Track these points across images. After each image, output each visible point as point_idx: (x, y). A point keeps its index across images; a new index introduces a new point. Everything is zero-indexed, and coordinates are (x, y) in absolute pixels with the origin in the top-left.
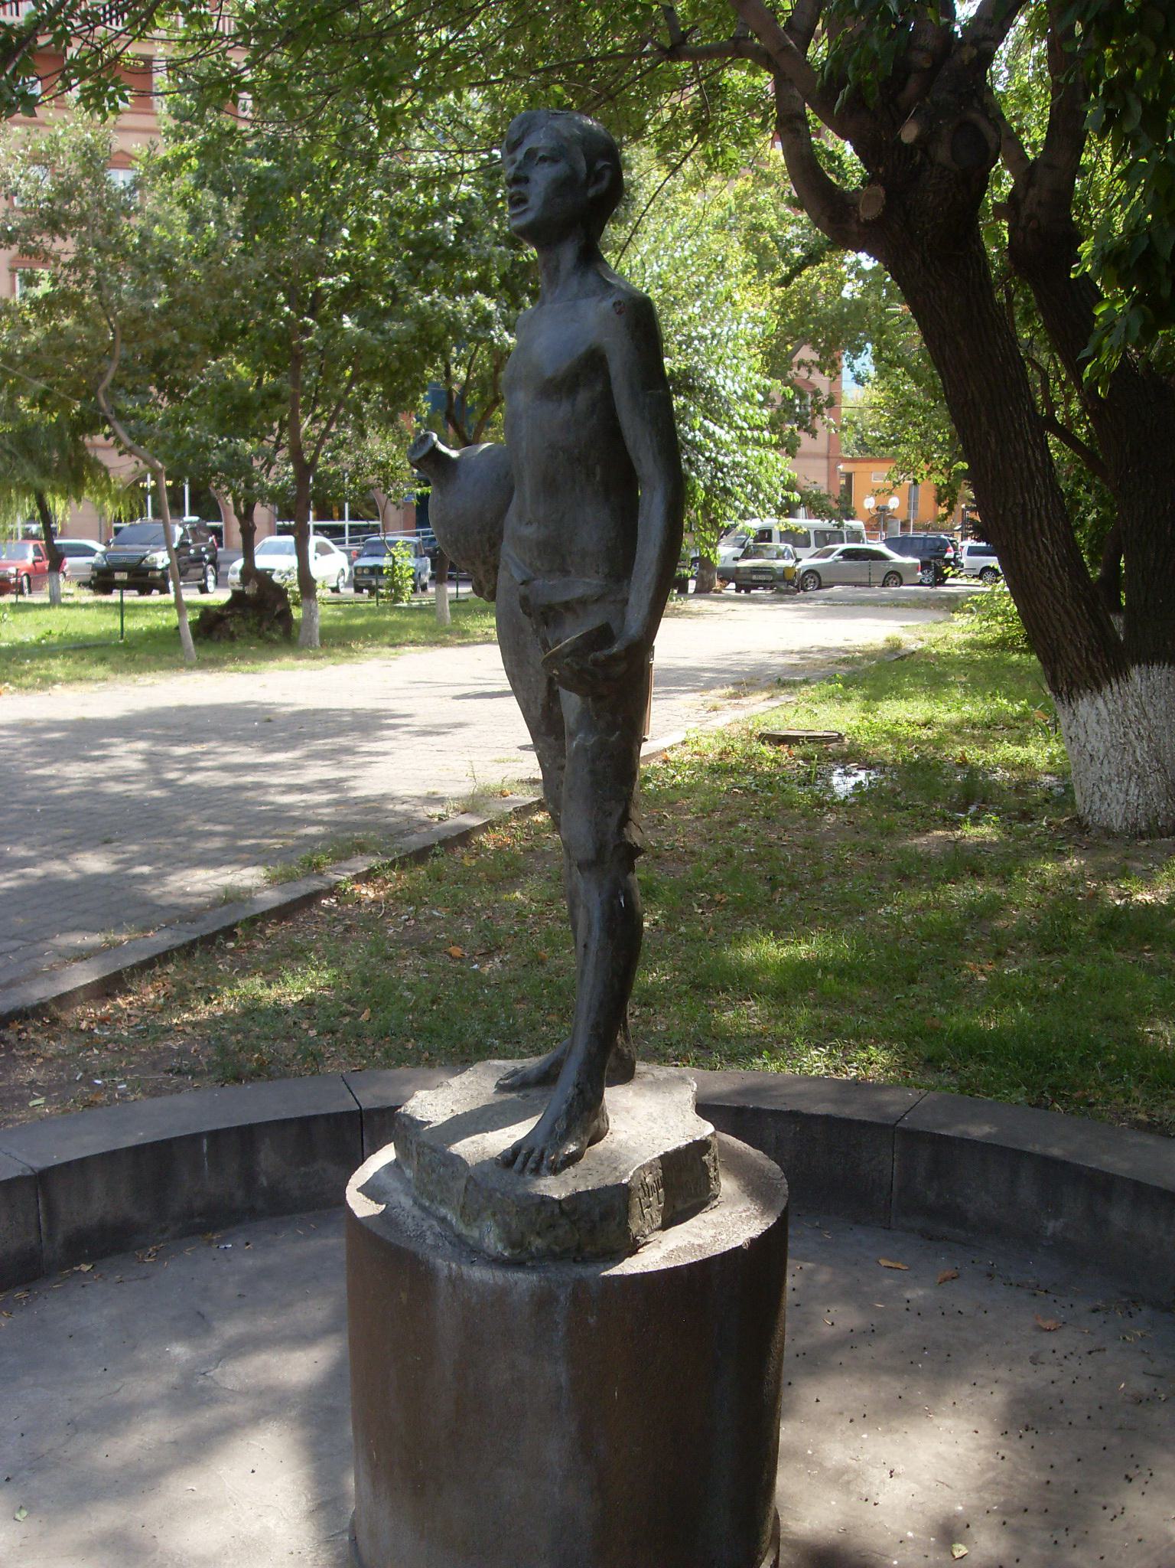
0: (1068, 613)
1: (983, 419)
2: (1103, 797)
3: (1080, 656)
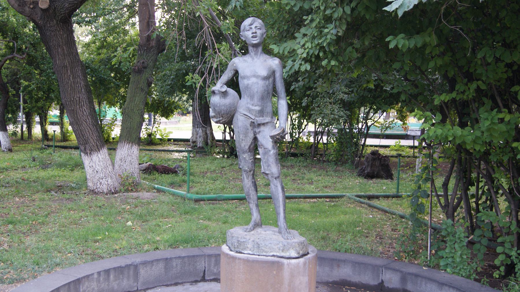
0: (91, 129)
1: (69, 71)
2: (101, 183)
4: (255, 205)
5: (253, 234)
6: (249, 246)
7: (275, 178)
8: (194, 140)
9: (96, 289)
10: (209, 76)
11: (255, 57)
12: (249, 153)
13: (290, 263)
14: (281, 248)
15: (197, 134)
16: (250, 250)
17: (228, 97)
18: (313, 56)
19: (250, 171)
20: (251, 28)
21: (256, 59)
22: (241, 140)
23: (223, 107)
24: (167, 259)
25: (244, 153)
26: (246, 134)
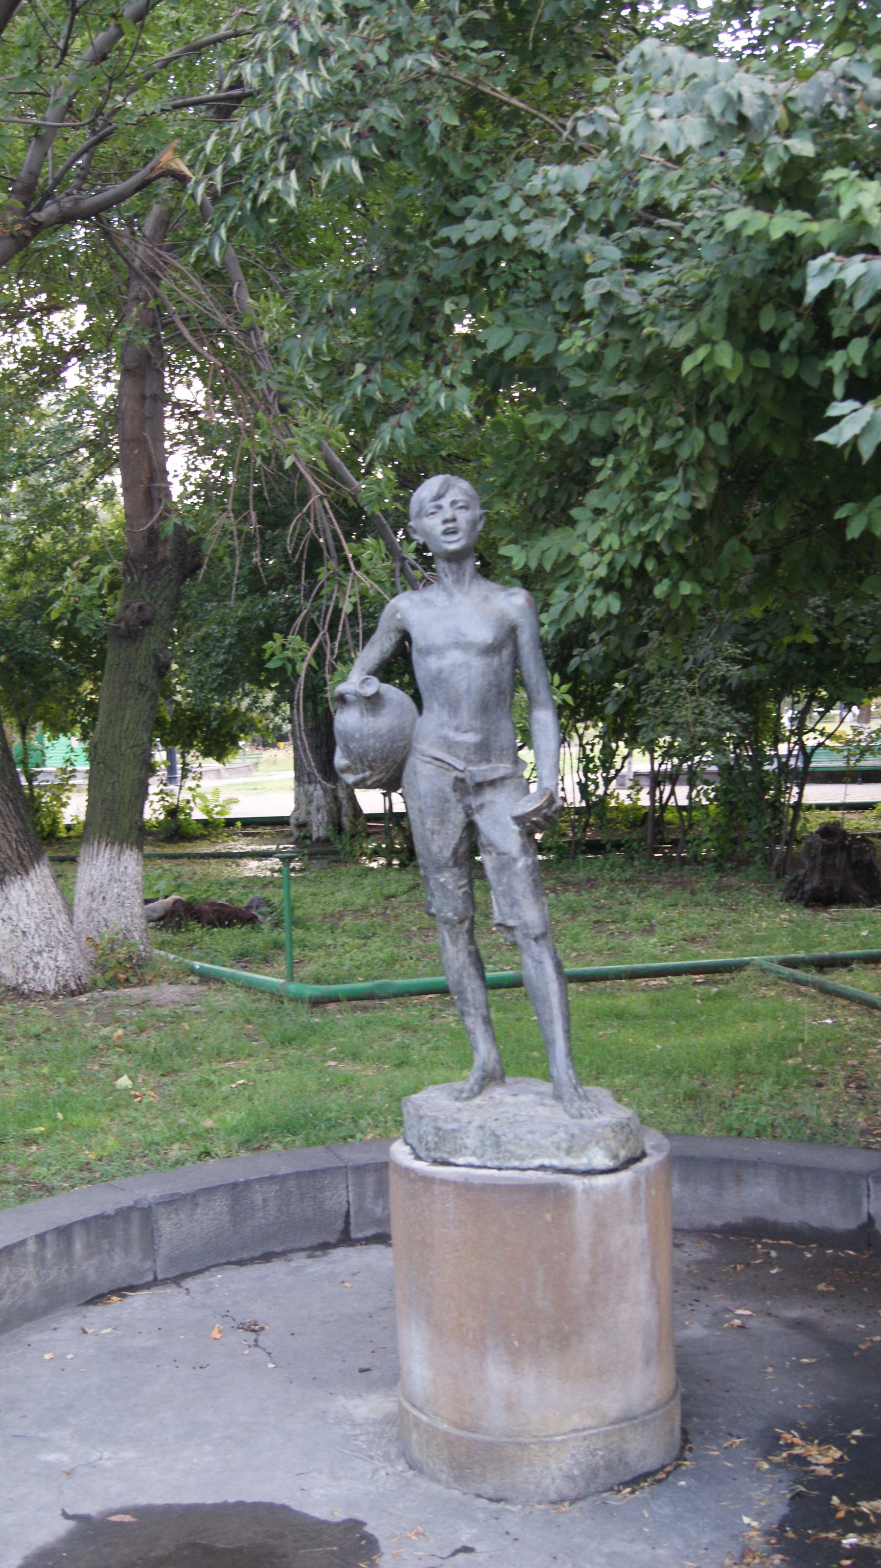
2: (36, 967)
3: (11, 848)
4: (480, 1020)
5: (480, 1107)
6: (471, 1142)
7: (536, 939)
8: (303, 818)
9: (35, 1284)
10: (333, 639)
11: (455, 591)
12: (456, 870)
13: (591, 1187)
14: (564, 1145)
15: (310, 802)
16: (474, 1154)
17: (385, 712)
18: (627, 572)
19: (461, 922)
20: (440, 507)
21: (458, 597)
23: (372, 741)
24: (235, 1185)
25: (439, 869)
26: (442, 816)
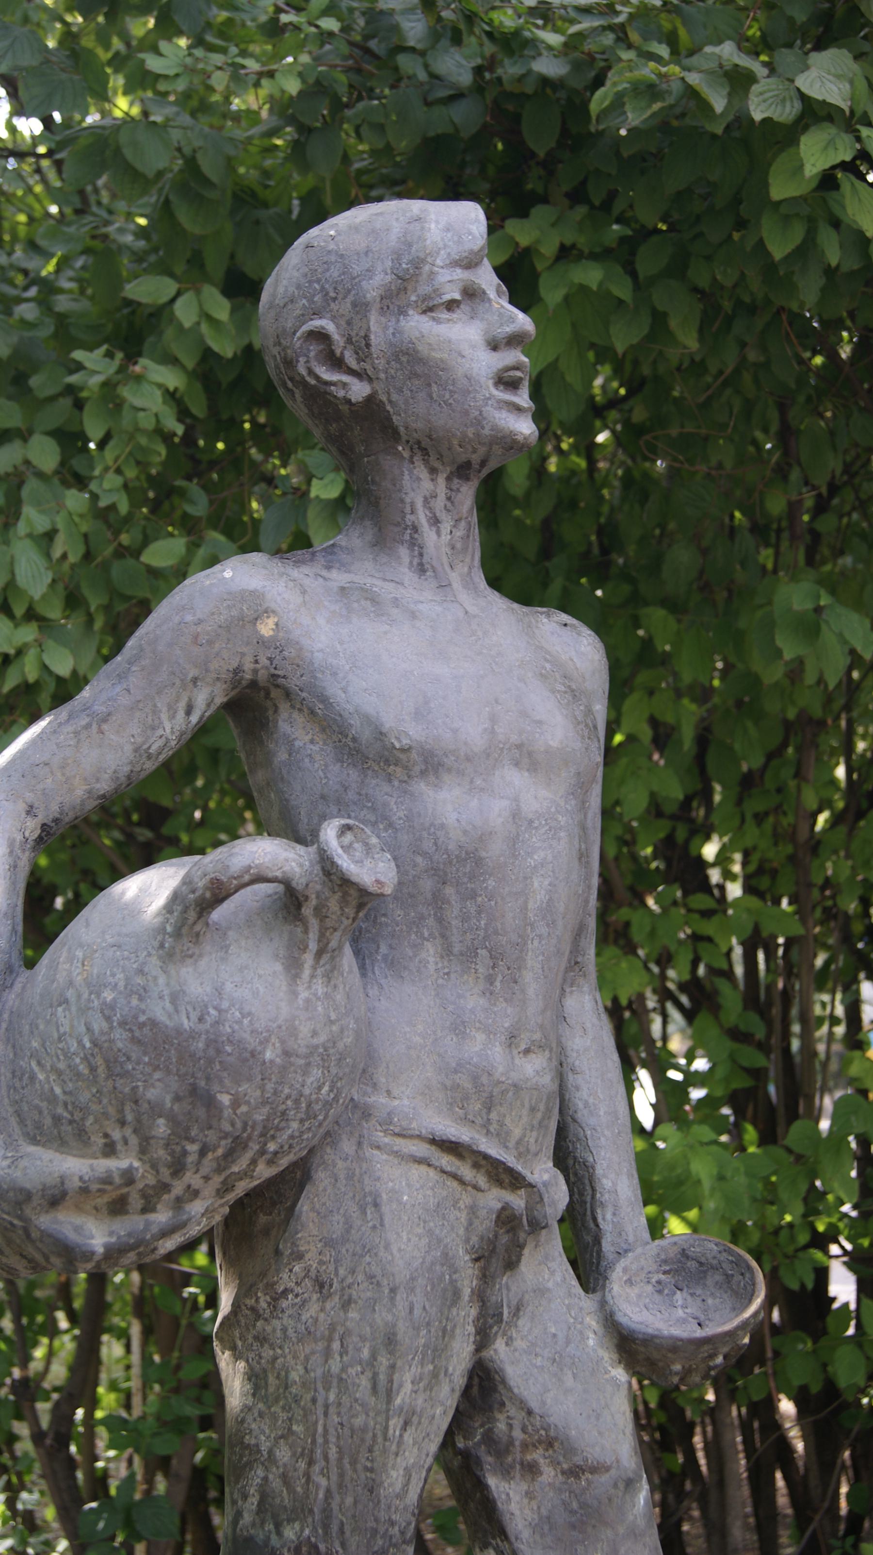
20: (472, 293)
22: (395, 1424)
26: (437, 1352)
